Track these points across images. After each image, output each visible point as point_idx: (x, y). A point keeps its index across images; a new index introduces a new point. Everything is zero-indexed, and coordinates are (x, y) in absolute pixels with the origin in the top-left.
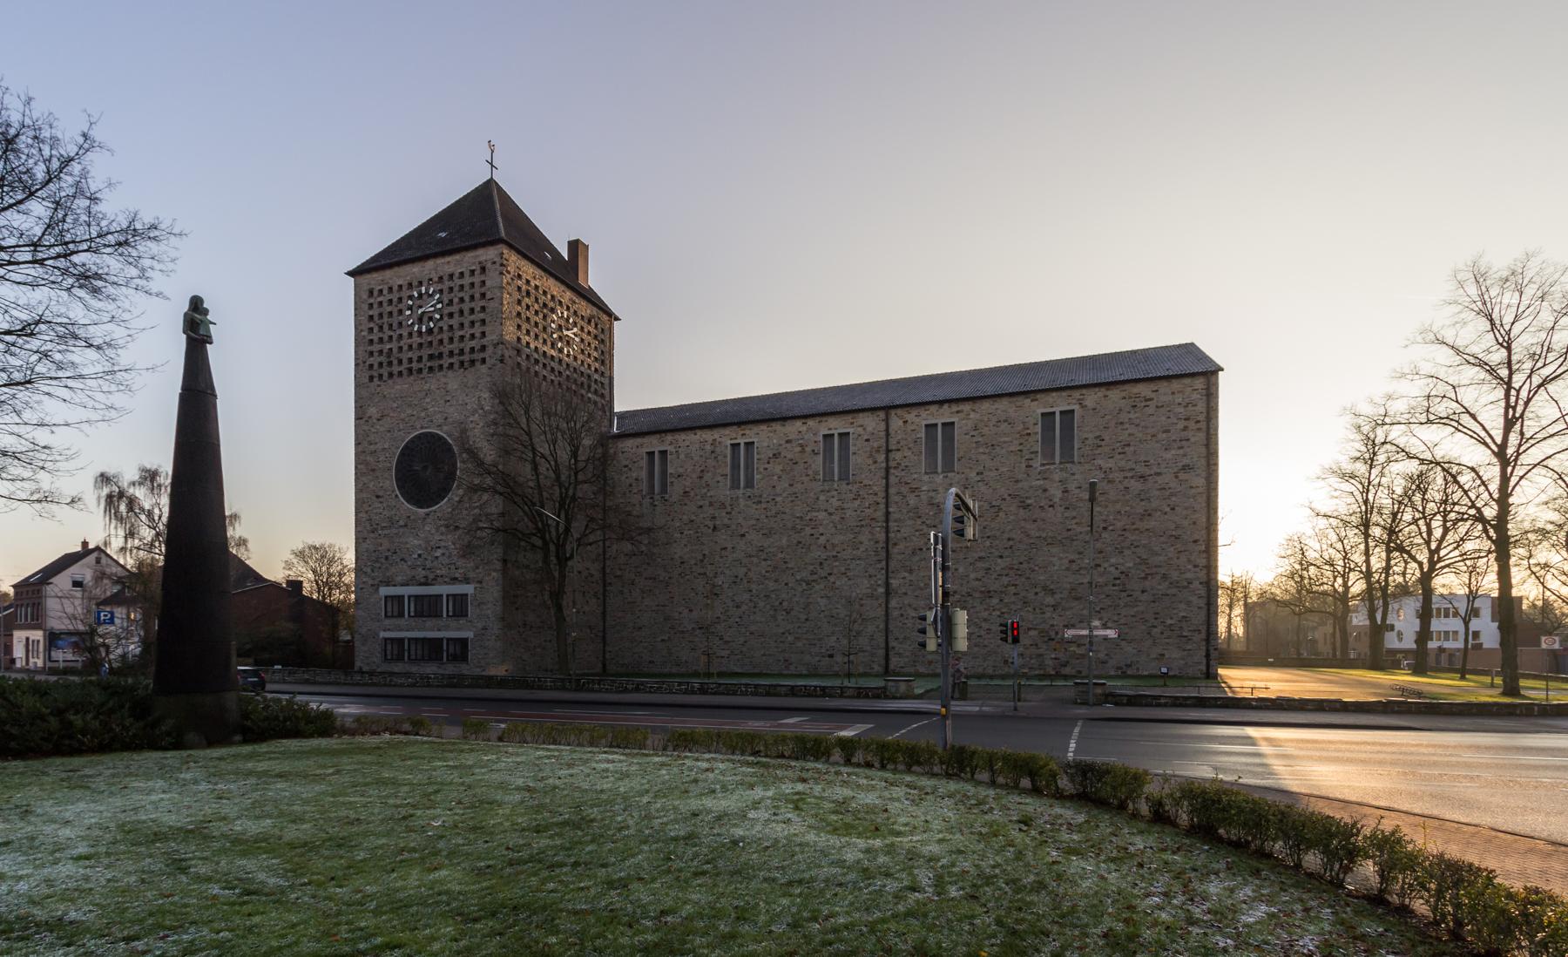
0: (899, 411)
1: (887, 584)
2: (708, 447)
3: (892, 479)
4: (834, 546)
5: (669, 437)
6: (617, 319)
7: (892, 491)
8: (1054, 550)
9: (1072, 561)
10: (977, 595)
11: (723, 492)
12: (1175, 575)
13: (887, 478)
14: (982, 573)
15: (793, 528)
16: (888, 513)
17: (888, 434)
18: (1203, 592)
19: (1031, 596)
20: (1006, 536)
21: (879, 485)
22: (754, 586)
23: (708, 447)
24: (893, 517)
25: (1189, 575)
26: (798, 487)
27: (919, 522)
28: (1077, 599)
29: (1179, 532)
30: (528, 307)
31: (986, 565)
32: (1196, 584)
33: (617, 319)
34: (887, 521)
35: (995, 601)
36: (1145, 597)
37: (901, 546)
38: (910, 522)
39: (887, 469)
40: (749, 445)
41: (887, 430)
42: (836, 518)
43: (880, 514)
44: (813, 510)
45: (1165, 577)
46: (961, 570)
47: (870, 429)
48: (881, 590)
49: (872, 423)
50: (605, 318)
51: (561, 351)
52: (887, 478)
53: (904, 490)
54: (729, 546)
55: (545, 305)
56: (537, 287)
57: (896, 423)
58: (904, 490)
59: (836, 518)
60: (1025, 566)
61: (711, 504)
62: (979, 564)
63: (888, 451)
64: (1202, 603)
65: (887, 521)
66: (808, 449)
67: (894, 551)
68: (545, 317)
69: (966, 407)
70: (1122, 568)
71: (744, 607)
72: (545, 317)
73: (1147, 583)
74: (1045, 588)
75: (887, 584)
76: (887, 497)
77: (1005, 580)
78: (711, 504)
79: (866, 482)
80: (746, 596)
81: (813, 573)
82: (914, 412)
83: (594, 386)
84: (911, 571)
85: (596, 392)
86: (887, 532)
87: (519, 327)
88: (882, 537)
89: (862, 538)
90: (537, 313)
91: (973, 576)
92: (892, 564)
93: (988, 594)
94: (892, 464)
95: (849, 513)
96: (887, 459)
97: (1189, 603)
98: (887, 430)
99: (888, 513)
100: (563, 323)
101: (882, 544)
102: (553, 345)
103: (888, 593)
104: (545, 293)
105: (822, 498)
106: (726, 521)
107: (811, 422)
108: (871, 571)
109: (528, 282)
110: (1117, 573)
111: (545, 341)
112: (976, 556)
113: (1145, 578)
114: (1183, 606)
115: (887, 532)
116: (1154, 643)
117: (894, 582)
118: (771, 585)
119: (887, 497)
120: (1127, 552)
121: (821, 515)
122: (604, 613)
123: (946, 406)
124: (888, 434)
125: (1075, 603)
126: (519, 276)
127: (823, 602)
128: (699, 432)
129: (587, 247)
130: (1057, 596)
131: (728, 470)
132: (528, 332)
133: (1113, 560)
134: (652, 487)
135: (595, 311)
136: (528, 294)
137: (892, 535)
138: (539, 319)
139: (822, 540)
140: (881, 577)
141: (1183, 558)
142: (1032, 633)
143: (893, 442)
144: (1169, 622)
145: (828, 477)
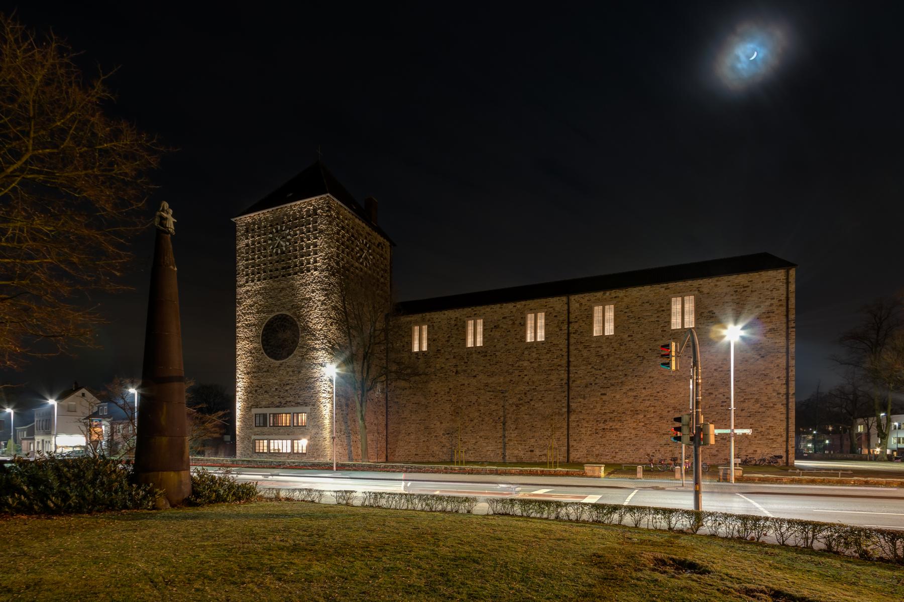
1: (568, 406)
3: (572, 341)
4: (533, 382)
7: (572, 348)
8: (681, 384)
12: (764, 399)
13: (568, 339)
14: (631, 399)
15: (507, 371)
16: (569, 362)
17: (569, 313)
18: (784, 411)
19: (665, 413)
20: (648, 375)
22: (481, 408)
23: (453, 322)
24: (572, 364)
25: (774, 400)
26: (510, 346)
27: (590, 367)
29: (768, 371)
31: (635, 394)
32: (779, 406)
34: (568, 366)
35: (641, 416)
37: (578, 382)
39: (569, 334)
41: (568, 310)
42: (536, 365)
43: (564, 362)
44: (520, 360)
45: (757, 401)
46: (618, 397)
47: (557, 309)
48: (565, 410)
52: (568, 339)
53: (580, 347)
54: (466, 383)
58: (580, 347)
59: (536, 365)
60: (661, 394)
61: (454, 357)
62: (630, 393)
63: (569, 323)
64: (784, 417)
65: (568, 366)
66: (517, 322)
67: (573, 385)
71: (476, 421)
73: (745, 405)
74: (674, 408)
75: (568, 406)
76: (568, 352)
77: (647, 403)
78: (454, 357)
79: (555, 342)
80: (477, 414)
81: (520, 399)
84: (584, 398)
86: (569, 373)
88: (565, 376)
89: (551, 377)
91: (626, 400)
92: (572, 394)
93: (636, 412)
95: (543, 362)
96: (568, 327)
97: (774, 417)
98: (568, 310)
99: (569, 362)
101: (565, 381)
105: (526, 352)
106: (464, 368)
108: (558, 398)
112: (628, 388)
114: (770, 419)
115: (569, 373)
117: (573, 405)
118: (493, 407)
119: (568, 352)
121: (526, 364)
122: (387, 425)
124: (569, 313)
127: (526, 417)
133: (721, 390)
139: (526, 379)
140: (565, 402)
141: (769, 387)
143: (572, 316)
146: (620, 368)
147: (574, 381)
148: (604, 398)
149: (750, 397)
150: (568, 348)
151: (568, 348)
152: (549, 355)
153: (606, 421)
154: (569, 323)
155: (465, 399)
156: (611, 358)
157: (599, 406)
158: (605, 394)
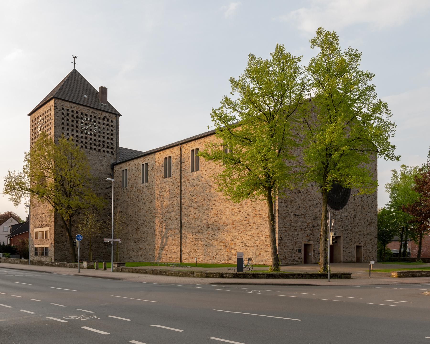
0: (184, 145)
2: (137, 166)
3: (183, 176)
5: (128, 163)
6: (120, 115)
7: (183, 181)
8: (227, 205)
9: (232, 210)
10: (205, 227)
11: (140, 185)
13: (181, 175)
16: (181, 191)
20: (213, 199)
21: (179, 180)
23: (137, 166)
24: (183, 192)
28: (234, 227)
30: (68, 120)
33: (120, 115)
34: (181, 195)
35: (210, 229)
36: (254, 226)
38: (187, 194)
40: (147, 164)
43: (179, 191)
47: (176, 154)
48: (180, 225)
49: (176, 150)
50: (114, 116)
51: (86, 133)
52: (181, 175)
54: (142, 208)
55: (77, 117)
56: (73, 111)
57: (183, 150)
60: (219, 212)
63: (181, 163)
65: (181, 195)
67: (183, 207)
68: (77, 122)
69: (202, 140)
70: (248, 213)
72: (77, 122)
74: (225, 222)
75: (181, 222)
79: (176, 177)
82: (188, 144)
83: (106, 145)
84: (187, 217)
85: (108, 147)
86: (181, 199)
87: (63, 128)
90: (72, 121)
92: (182, 213)
94: (182, 169)
99: (181, 191)
100: (87, 122)
101: (180, 205)
102: (82, 132)
103: (181, 227)
104: (77, 113)
106: (141, 198)
107: (161, 152)
109: (68, 110)
110: (246, 215)
111: (77, 131)
112: (205, 209)
113: (255, 217)
115: (181, 199)
116: (257, 249)
119: (181, 184)
120: (249, 204)
123: (197, 140)
125: (233, 230)
126: (63, 109)
128: (135, 160)
129: (106, 89)
130: (228, 226)
131: (141, 176)
132: (68, 129)
134: (123, 184)
135: (107, 114)
136: (68, 115)
137: (182, 200)
138: (75, 123)
142: (221, 244)
144: (262, 238)
145: (166, 177)
146: (202, 194)
147: (183, 205)
148: (195, 215)
149: (257, 213)
150: (181, 181)
151: (181, 181)
152: (173, 186)
153: (196, 233)
154: (181, 163)
155: (141, 219)
156: (198, 187)
157: (193, 221)
158: (195, 214)
